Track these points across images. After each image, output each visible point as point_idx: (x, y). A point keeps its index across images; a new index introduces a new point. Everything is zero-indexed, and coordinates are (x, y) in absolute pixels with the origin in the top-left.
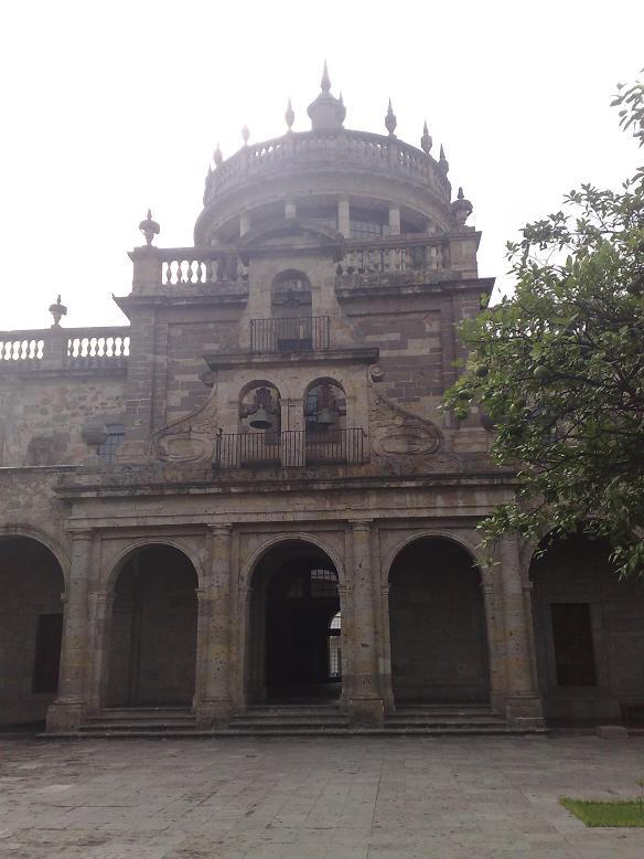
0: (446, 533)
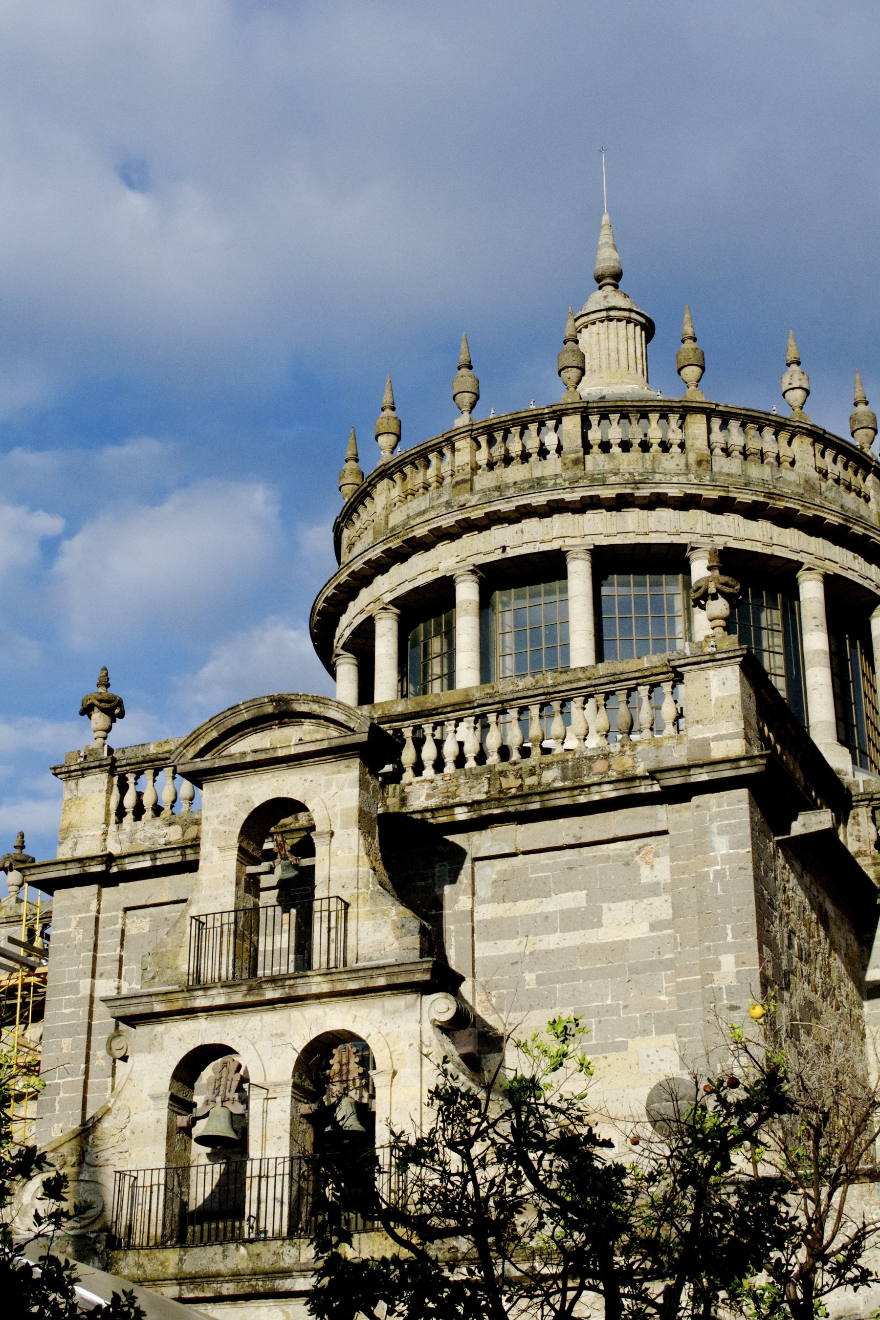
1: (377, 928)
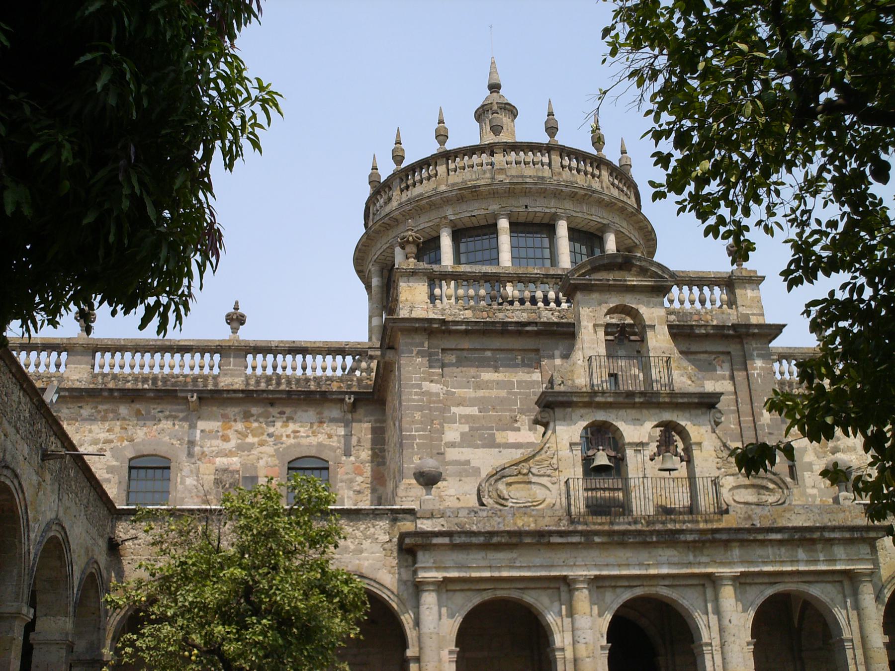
0: (804, 587)
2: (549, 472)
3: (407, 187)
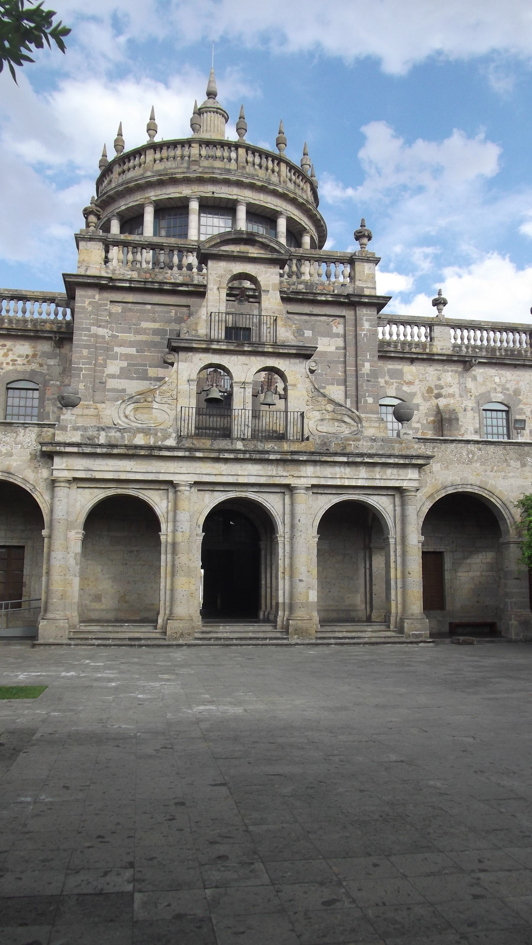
1: (287, 331)
2: (170, 401)
3: (124, 172)
